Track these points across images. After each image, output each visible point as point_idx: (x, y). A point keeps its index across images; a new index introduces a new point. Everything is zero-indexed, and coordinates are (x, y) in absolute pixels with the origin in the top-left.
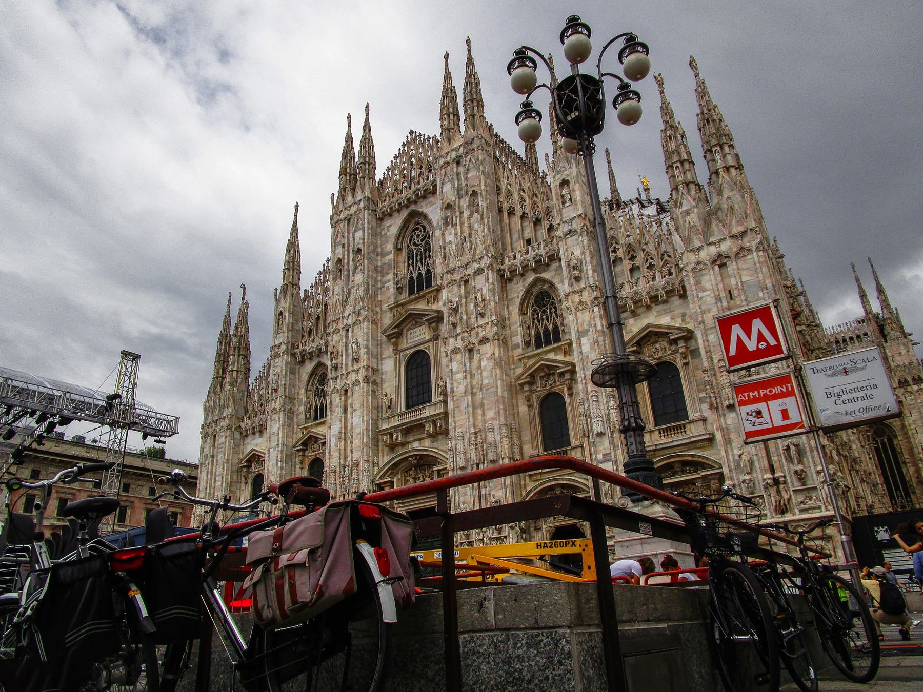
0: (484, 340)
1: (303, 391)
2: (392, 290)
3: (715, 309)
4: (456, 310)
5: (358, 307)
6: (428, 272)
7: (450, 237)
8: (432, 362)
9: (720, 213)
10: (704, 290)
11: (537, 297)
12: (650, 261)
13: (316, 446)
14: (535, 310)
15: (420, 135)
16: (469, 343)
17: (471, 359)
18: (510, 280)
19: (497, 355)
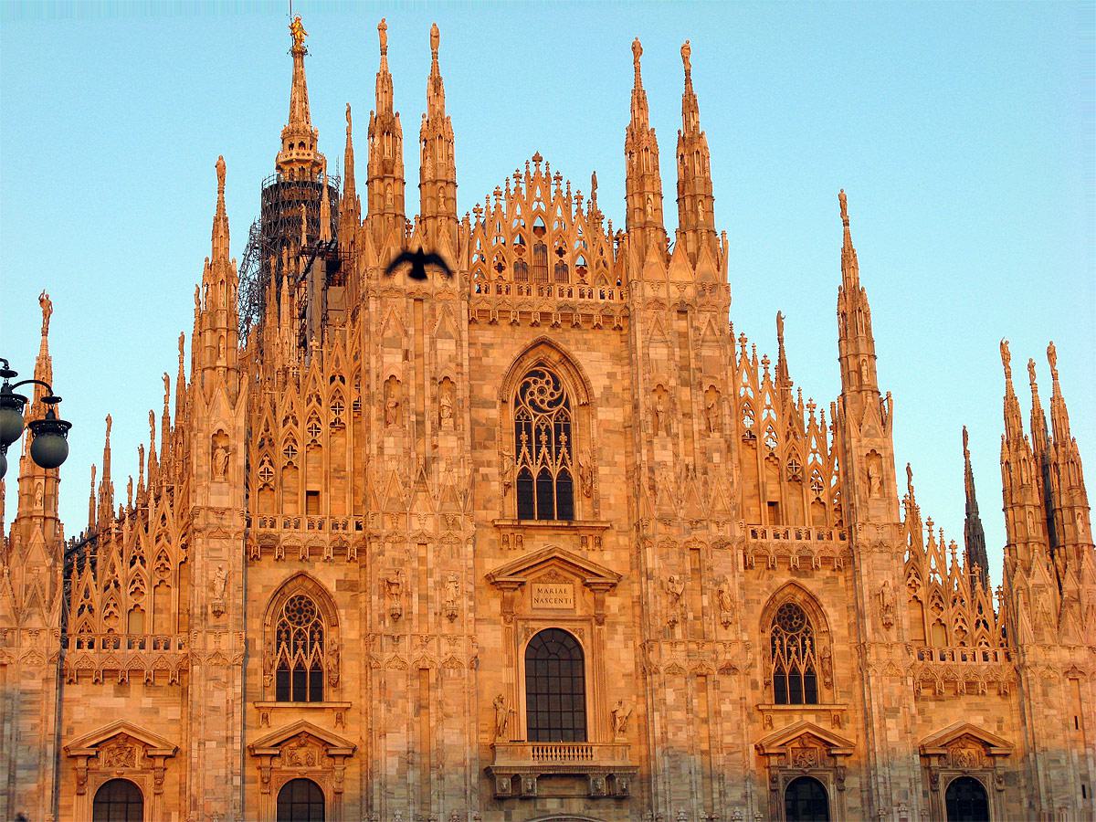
0: (729, 669)
1: (255, 624)
2: (496, 487)
3: (1061, 737)
4: (678, 597)
5: (450, 508)
8: (588, 661)
9: (1076, 606)
10: (1051, 707)
11: (781, 610)
12: (960, 623)
13: (301, 753)
14: (776, 631)
15: (558, 178)
16: (701, 666)
17: (702, 688)
18: (751, 567)
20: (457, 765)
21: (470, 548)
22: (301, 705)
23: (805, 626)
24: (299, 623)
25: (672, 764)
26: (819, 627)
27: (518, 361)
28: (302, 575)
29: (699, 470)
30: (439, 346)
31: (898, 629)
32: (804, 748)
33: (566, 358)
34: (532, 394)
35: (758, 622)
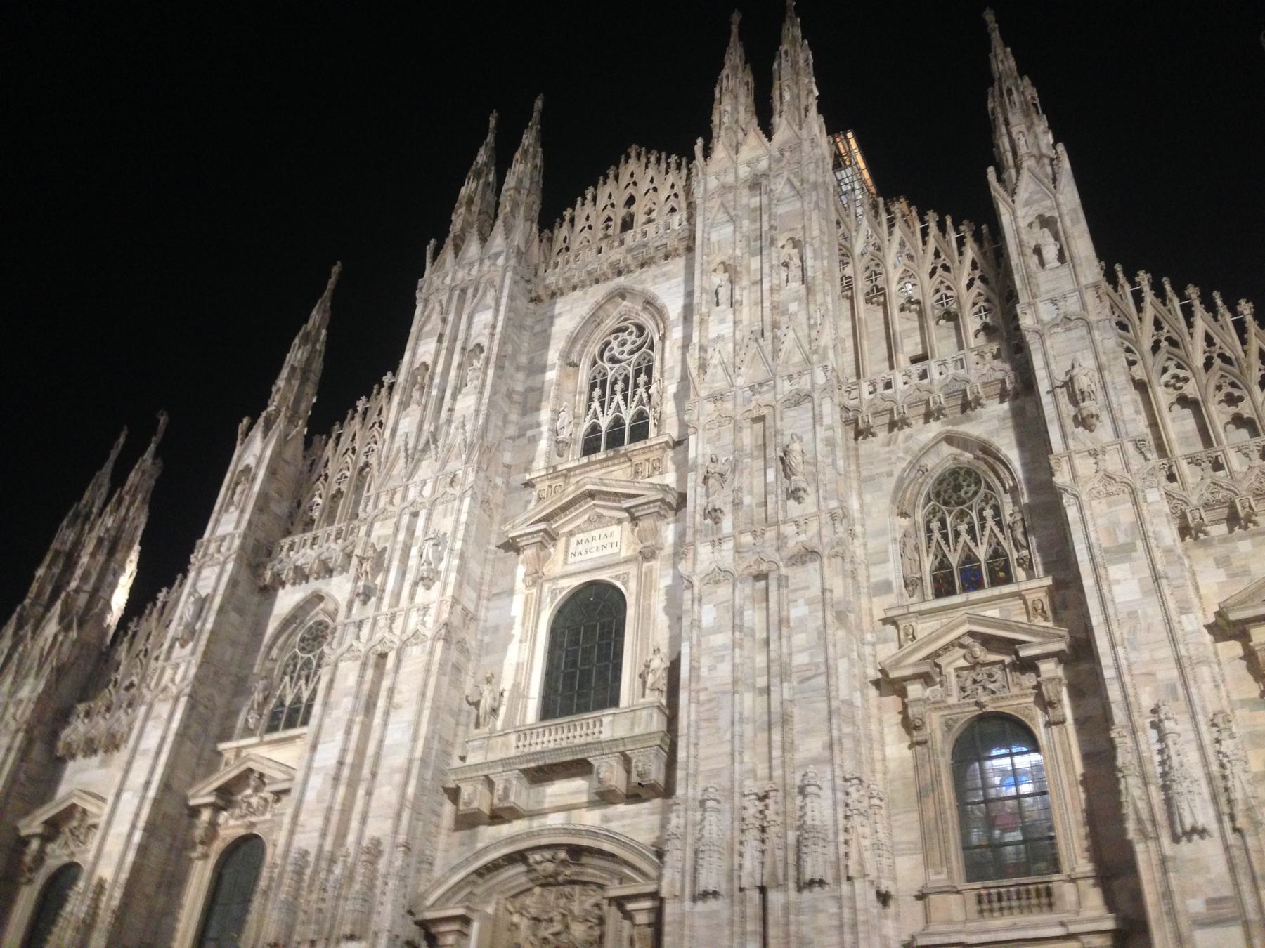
6: (641, 415)
7: (719, 326)
8: (631, 612)
11: (940, 481)
14: (934, 512)
19: (838, 593)
20: (394, 771)
21: (467, 501)
22: (267, 738)
23: (983, 491)
24: (310, 652)
25: (704, 716)
26: (1003, 485)
27: (594, 319)
28: (318, 598)
29: (768, 328)
30: (476, 319)
31: (1114, 422)
32: (975, 665)
33: (650, 303)
34: (612, 349)
35: (887, 500)
